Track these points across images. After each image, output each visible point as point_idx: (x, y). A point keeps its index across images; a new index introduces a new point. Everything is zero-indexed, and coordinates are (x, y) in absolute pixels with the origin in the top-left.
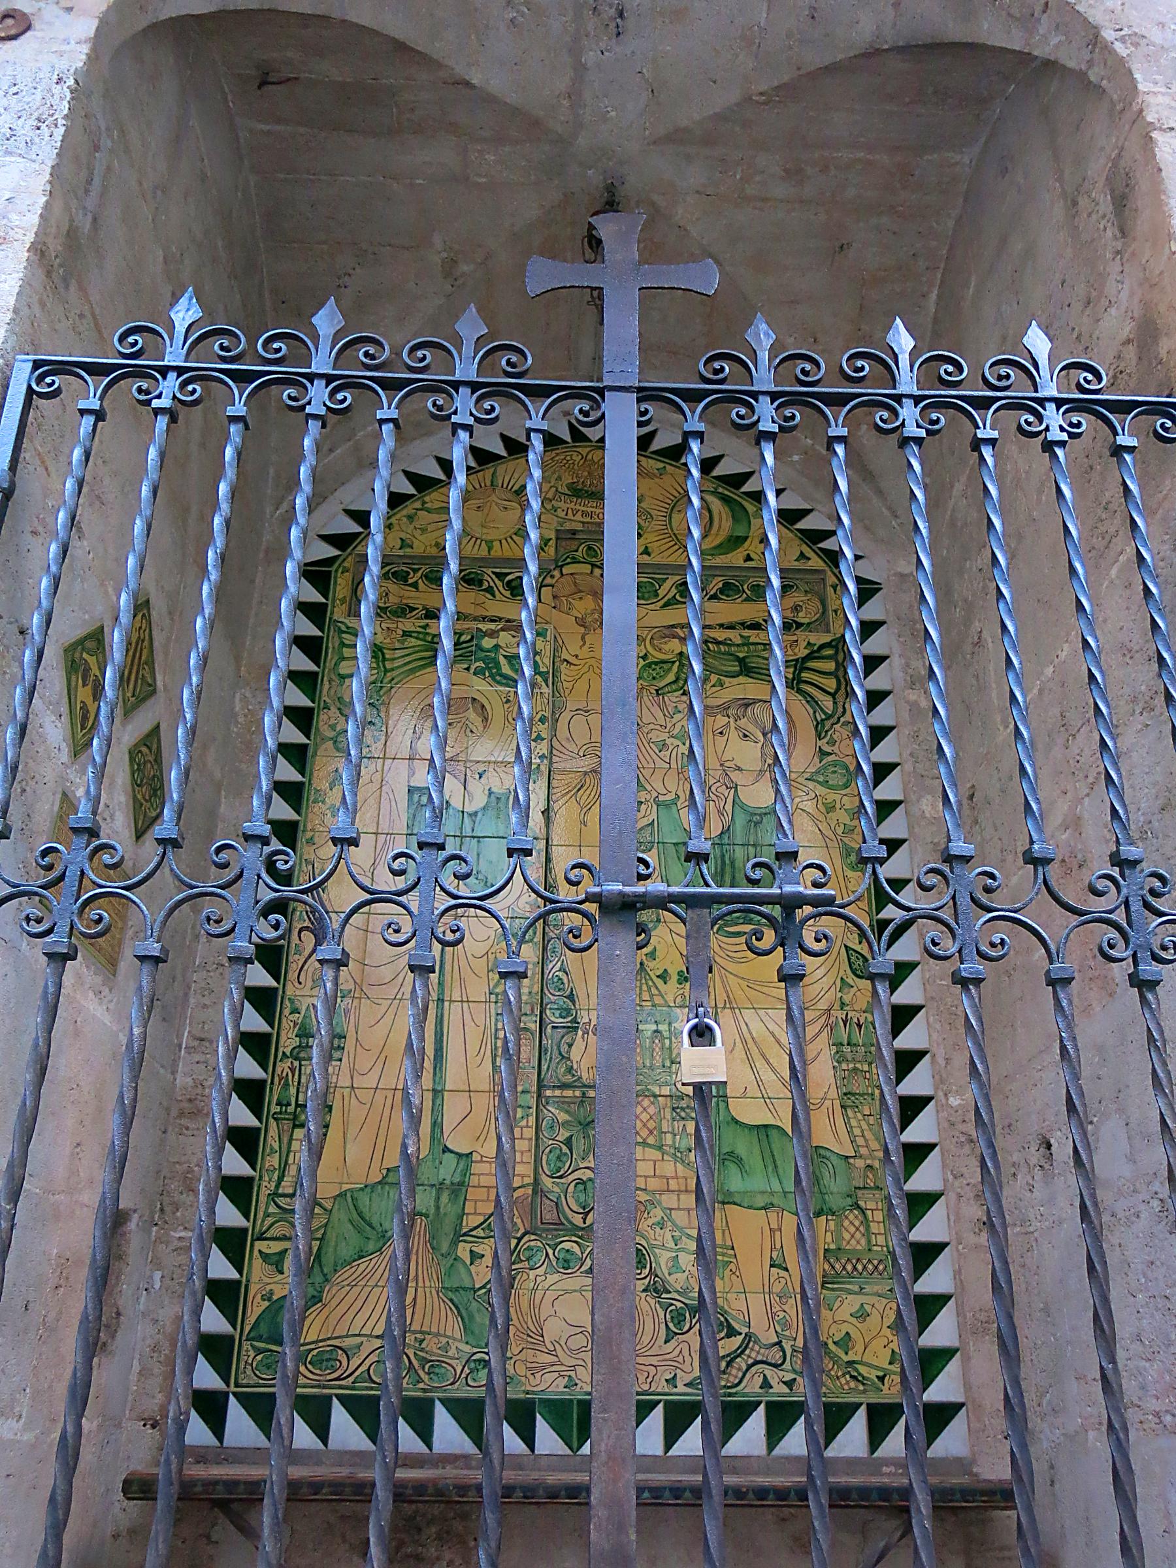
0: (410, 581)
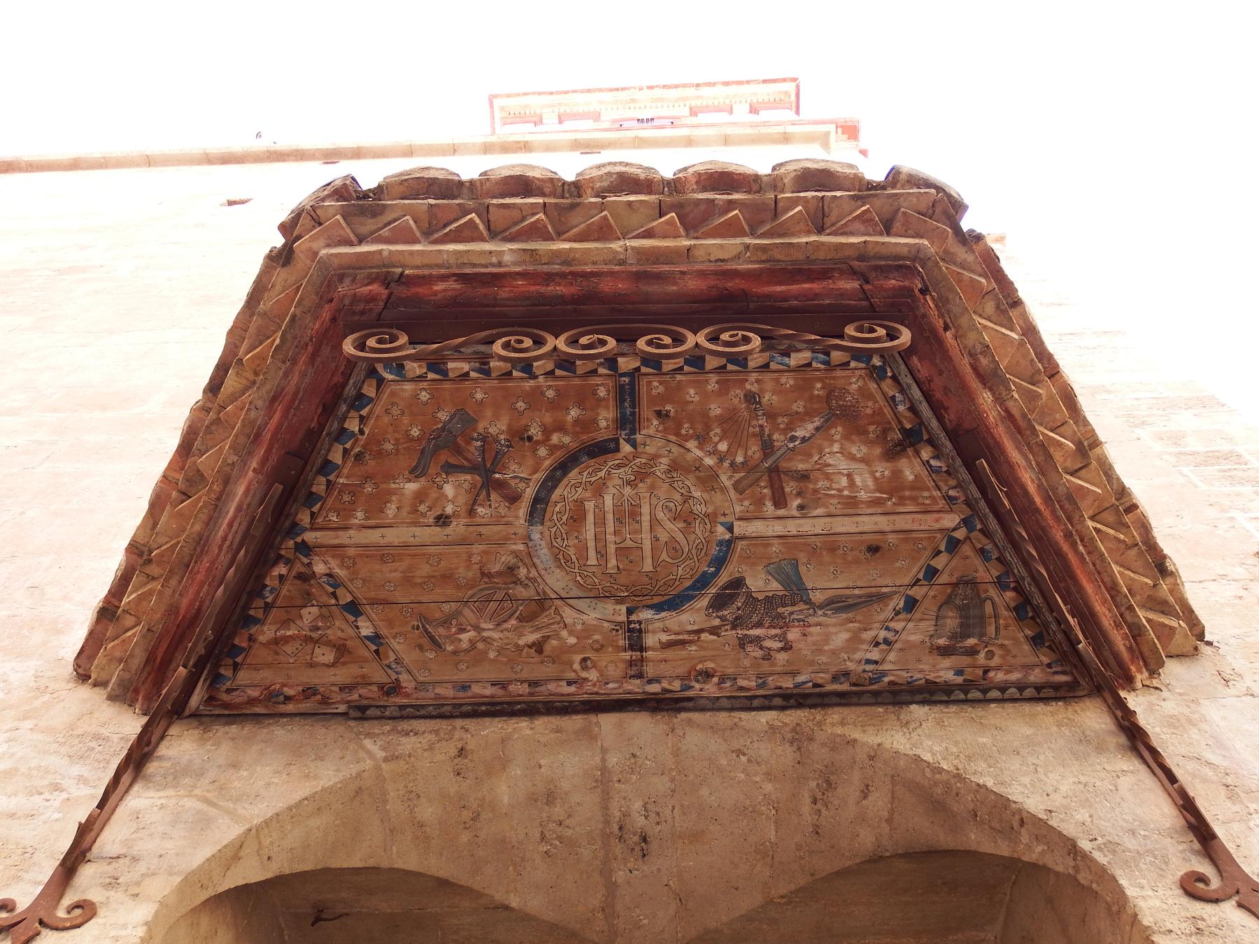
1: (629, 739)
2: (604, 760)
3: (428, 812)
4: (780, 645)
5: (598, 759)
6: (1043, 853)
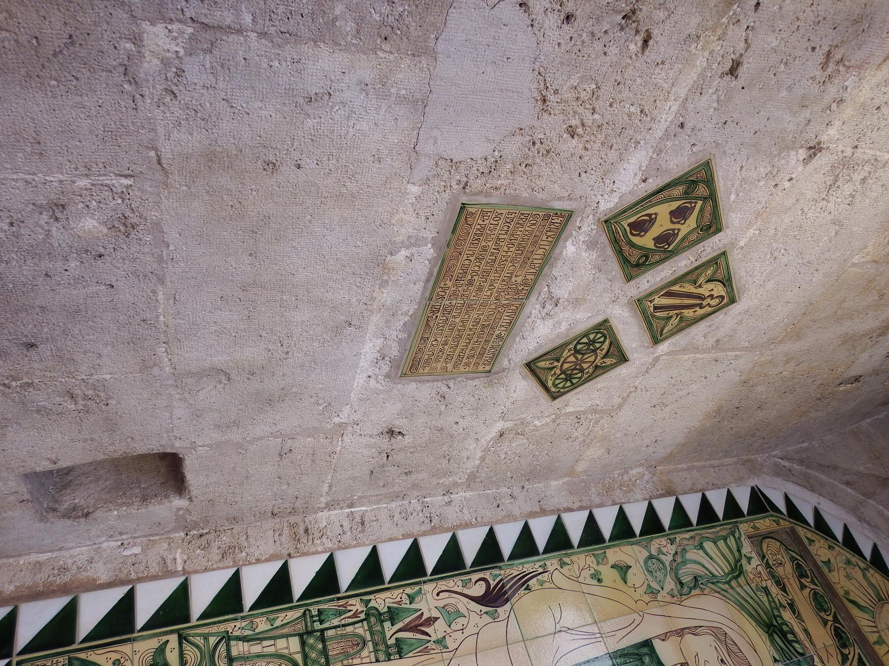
0: (803, 580)
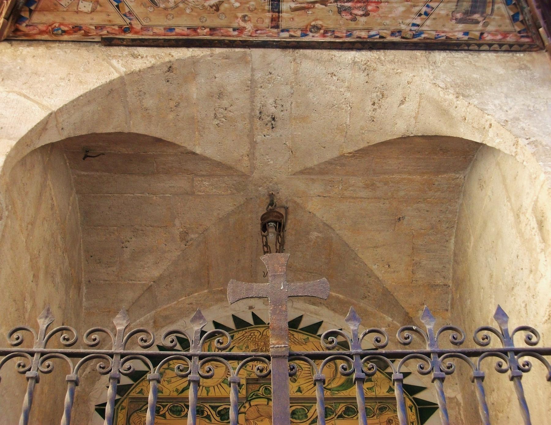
0: (161, 413)
1: (269, 64)
2: (252, 75)
3: (149, 102)
4: (361, 13)
5: (249, 75)
6: (499, 143)
